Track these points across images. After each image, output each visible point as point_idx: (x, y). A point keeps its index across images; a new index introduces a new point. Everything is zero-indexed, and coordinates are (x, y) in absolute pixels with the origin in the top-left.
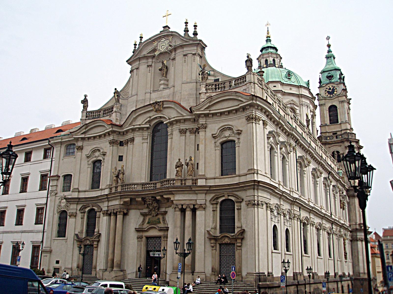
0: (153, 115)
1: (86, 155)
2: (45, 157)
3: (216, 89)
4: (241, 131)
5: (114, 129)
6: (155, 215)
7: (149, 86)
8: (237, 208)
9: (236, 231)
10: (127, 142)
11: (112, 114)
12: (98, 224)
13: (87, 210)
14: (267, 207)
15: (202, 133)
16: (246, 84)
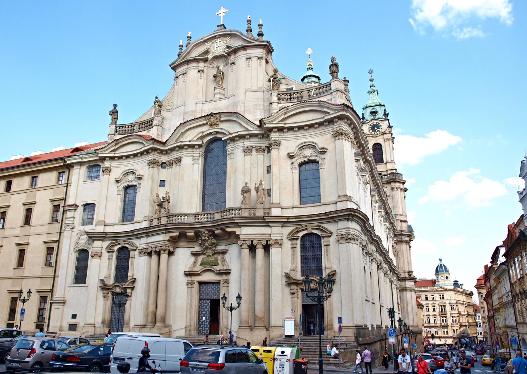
0: (206, 129)
3: (290, 99)
4: (327, 149)
5: (155, 146)
6: (211, 254)
8: (325, 244)
10: (170, 164)
13: (116, 248)
15: (274, 152)
16: (331, 93)
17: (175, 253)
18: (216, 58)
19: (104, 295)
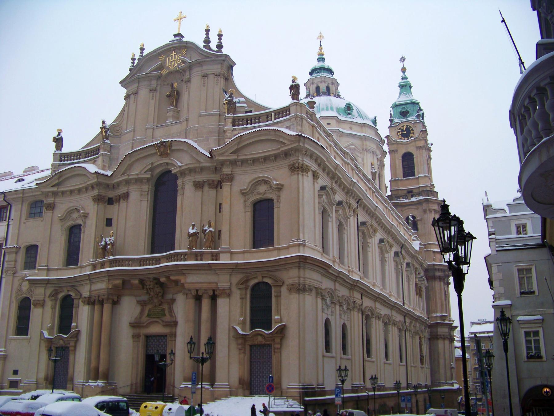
4: (282, 185)
9: (275, 327)
13: (61, 295)
14: (317, 293)
15: (226, 188)
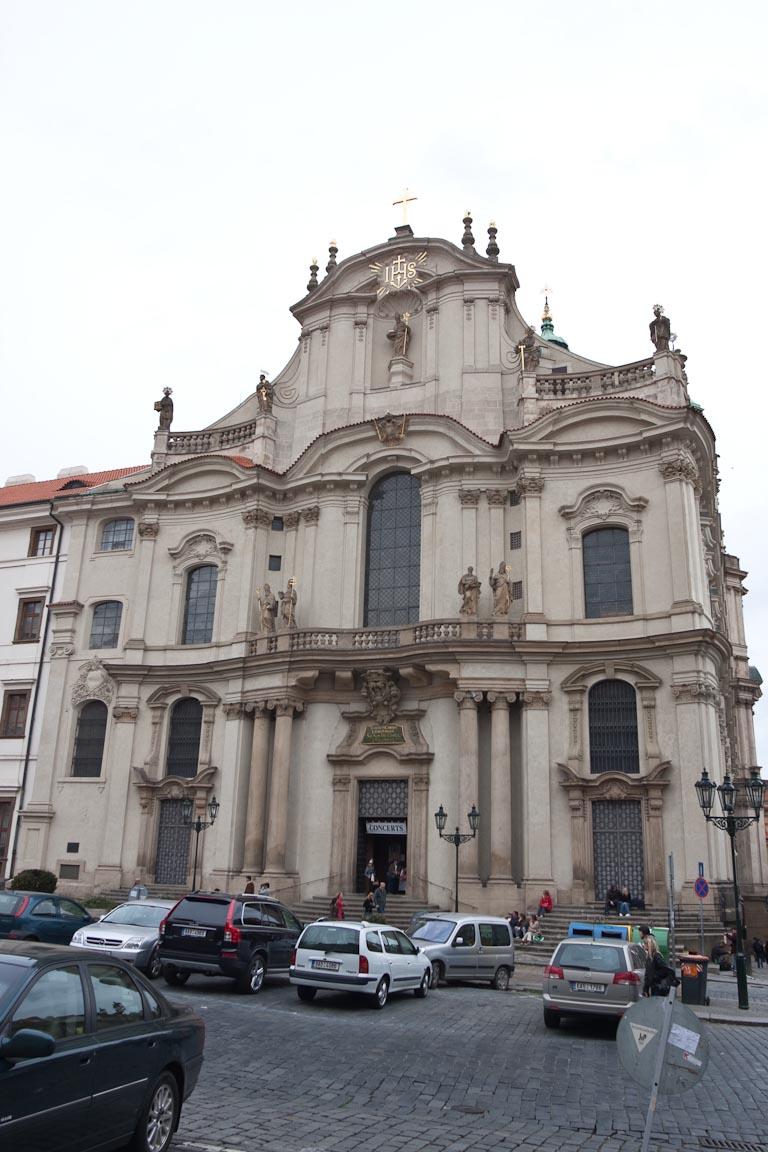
0: (376, 450)
1: (169, 549)
2: (33, 551)
4: (647, 501)
5: (261, 481)
6: (387, 719)
7: (359, 373)
8: (646, 703)
9: (645, 768)
10: (294, 521)
11: (253, 441)
12: (207, 742)
13: (171, 700)
15: (530, 505)
16: (655, 382)
17: (307, 715)
18: (395, 296)
19: (143, 801)
